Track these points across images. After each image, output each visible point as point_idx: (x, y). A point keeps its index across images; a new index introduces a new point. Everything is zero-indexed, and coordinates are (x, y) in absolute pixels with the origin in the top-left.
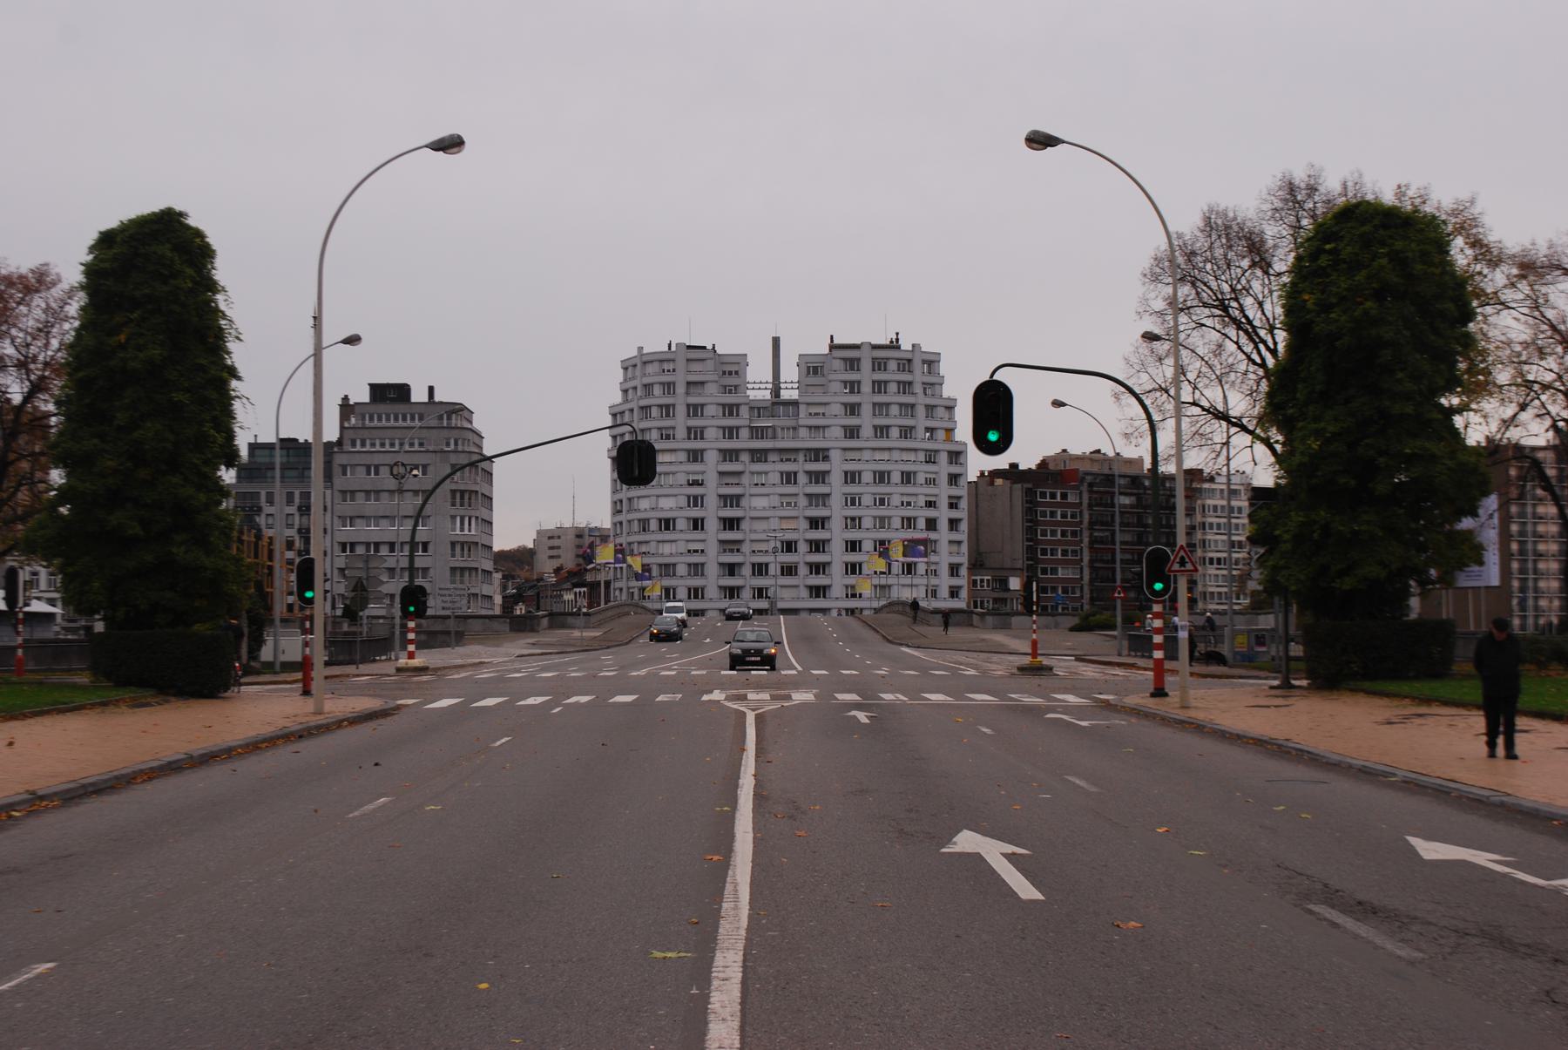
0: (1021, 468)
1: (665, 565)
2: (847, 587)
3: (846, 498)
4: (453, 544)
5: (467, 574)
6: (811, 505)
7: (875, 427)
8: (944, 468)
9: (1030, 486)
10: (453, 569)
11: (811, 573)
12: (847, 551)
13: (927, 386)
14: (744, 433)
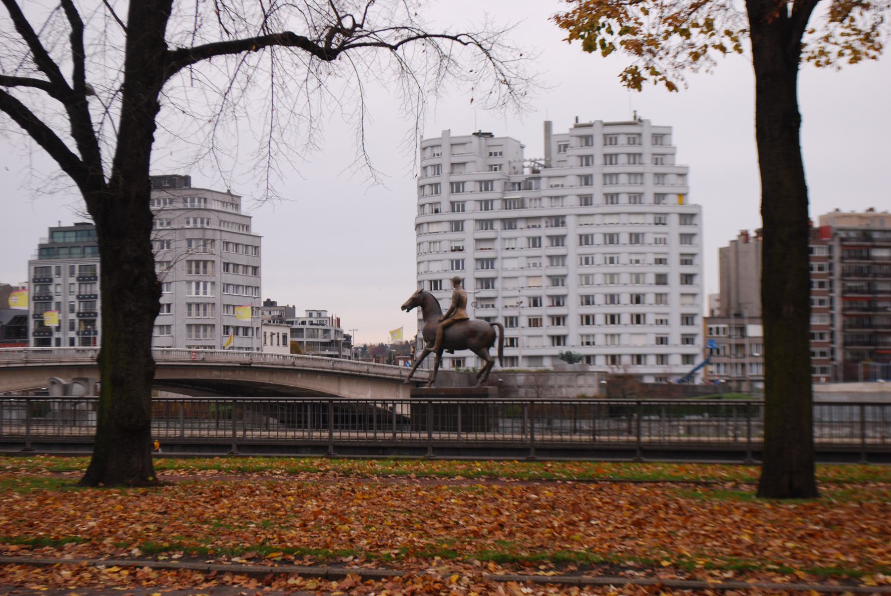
2: (582, 336)
3: (581, 258)
4: (189, 305)
5: (202, 329)
6: (552, 265)
7: (606, 195)
8: (674, 228)
10: (189, 326)
11: (553, 324)
13: (658, 159)
14: (497, 205)
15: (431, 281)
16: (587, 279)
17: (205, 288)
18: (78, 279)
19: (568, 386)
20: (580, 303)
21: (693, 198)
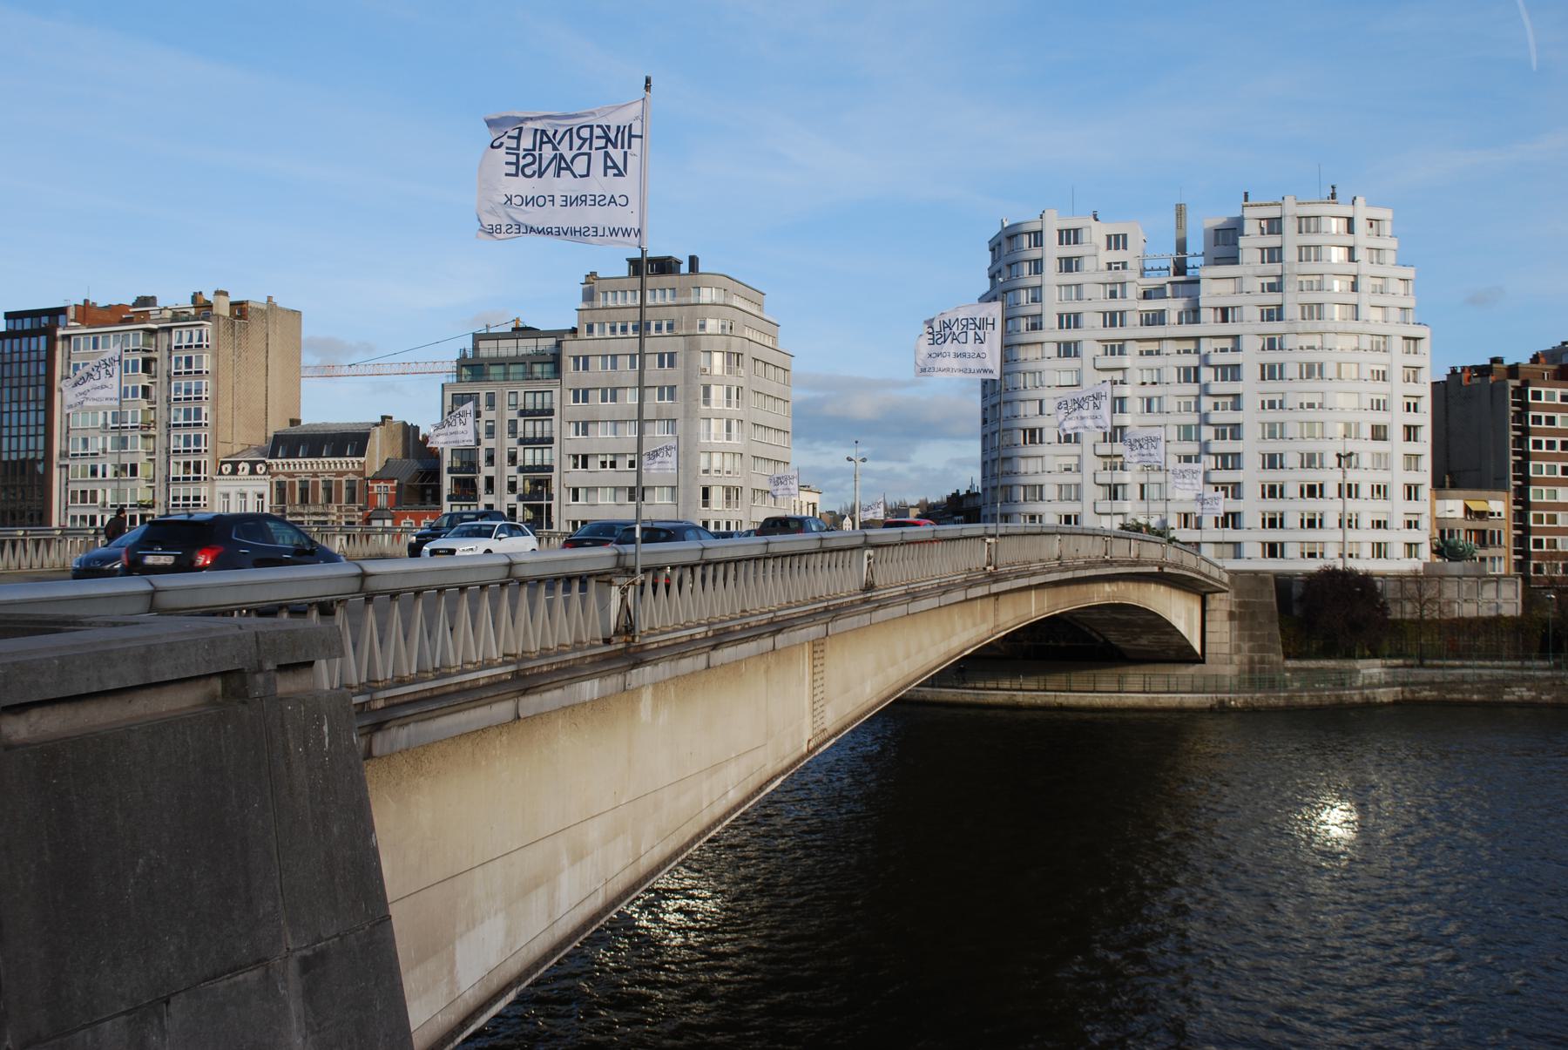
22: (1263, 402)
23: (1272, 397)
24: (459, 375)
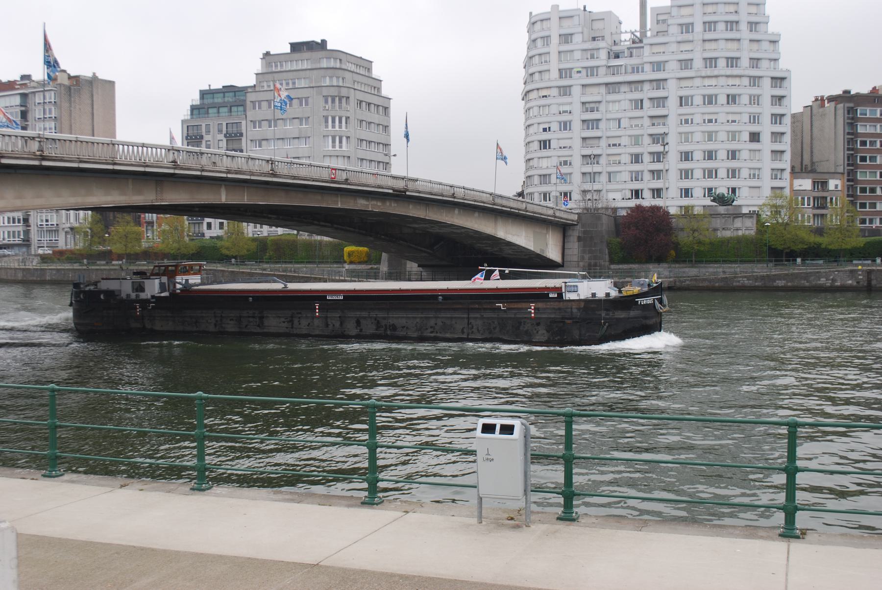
0: (852, 93)
1: (544, 175)
8: (767, 90)
9: (851, 105)
11: (654, 179)
12: (681, 161)
13: (753, 26)
15: (540, 142)
16: (686, 137)
17: (341, 142)
18: (225, 136)
19: (724, 229)
20: (679, 160)
21: (783, 64)
22: (681, 120)
23: (686, 117)
24: (192, 114)
